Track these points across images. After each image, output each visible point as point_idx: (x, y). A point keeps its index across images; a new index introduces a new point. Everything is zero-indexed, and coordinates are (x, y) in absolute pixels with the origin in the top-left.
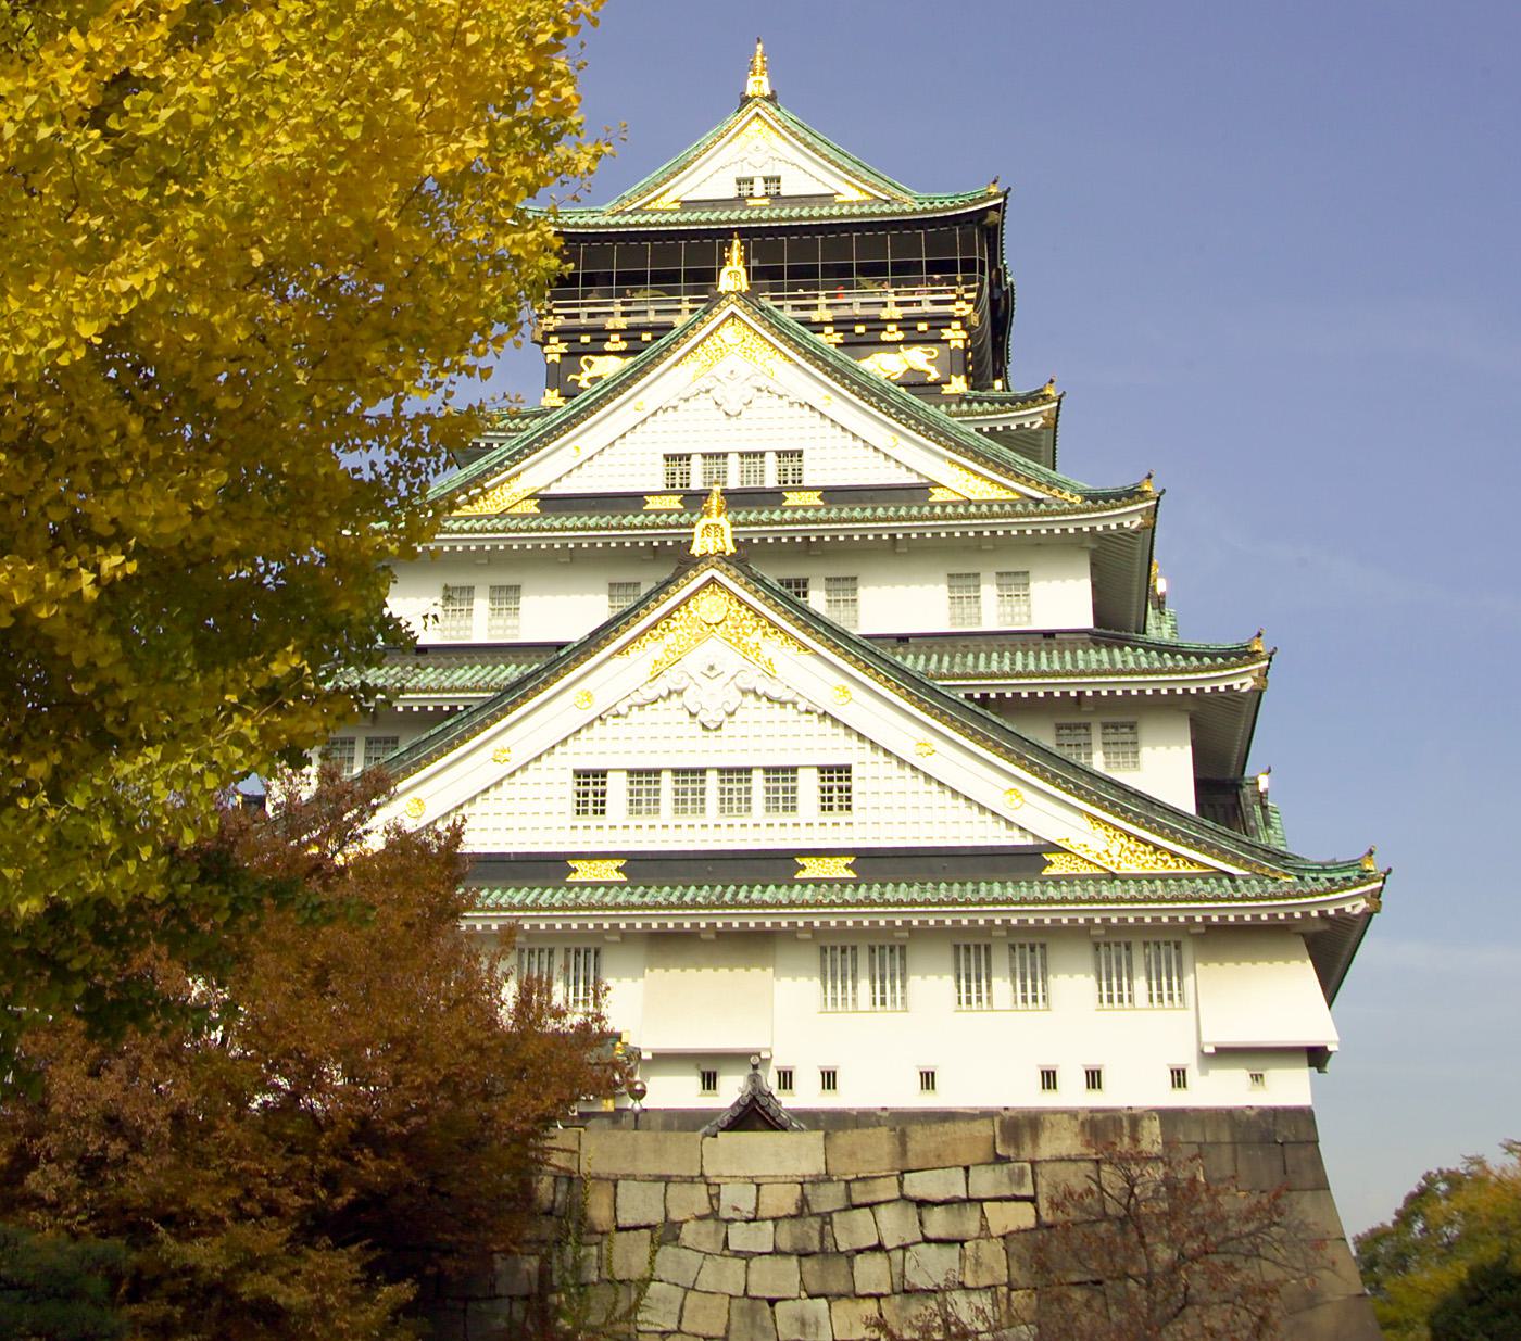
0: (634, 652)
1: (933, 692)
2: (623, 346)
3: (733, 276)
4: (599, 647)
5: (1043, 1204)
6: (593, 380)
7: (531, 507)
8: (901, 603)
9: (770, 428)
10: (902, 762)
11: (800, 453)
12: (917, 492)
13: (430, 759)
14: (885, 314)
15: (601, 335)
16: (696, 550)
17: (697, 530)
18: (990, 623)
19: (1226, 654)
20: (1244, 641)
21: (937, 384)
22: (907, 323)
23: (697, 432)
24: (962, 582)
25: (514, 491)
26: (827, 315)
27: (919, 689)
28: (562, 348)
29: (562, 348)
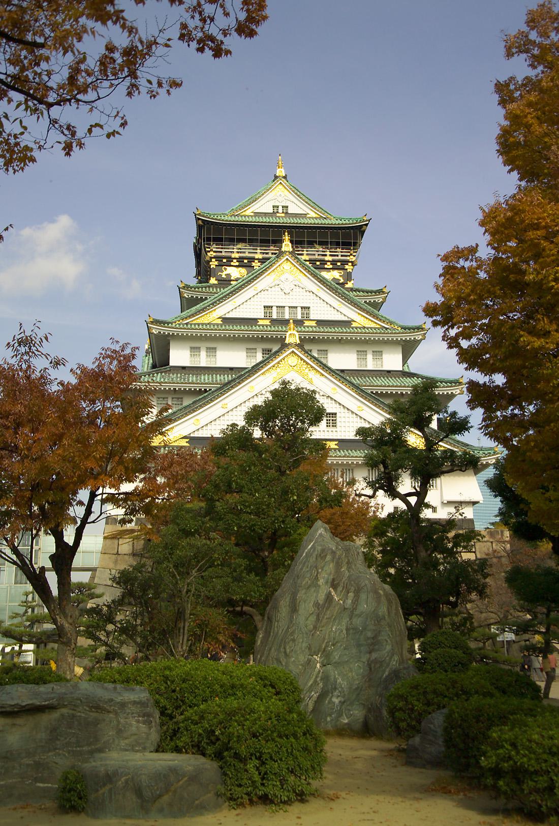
0: (267, 374)
1: (362, 391)
2: (237, 264)
3: (287, 246)
4: (256, 372)
5: (478, 553)
6: (228, 275)
7: (219, 321)
8: (343, 359)
9: (299, 299)
10: (353, 412)
11: (309, 308)
12: (347, 323)
13: (201, 407)
14: (327, 258)
15: (230, 259)
16: (287, 342)
17: (288, 334)
18: (370, 367)
19: (451, 382)
20: (457, 378)
21: (342, 285)
22: (334, 262)
23: (275, 299)
24: (362, 354)
25: (214, 316)
26: (307, 258)
27: (358, 389)
28: (216, 263)
29: (216, 263)
